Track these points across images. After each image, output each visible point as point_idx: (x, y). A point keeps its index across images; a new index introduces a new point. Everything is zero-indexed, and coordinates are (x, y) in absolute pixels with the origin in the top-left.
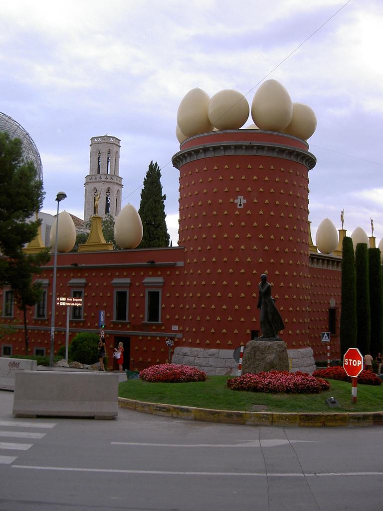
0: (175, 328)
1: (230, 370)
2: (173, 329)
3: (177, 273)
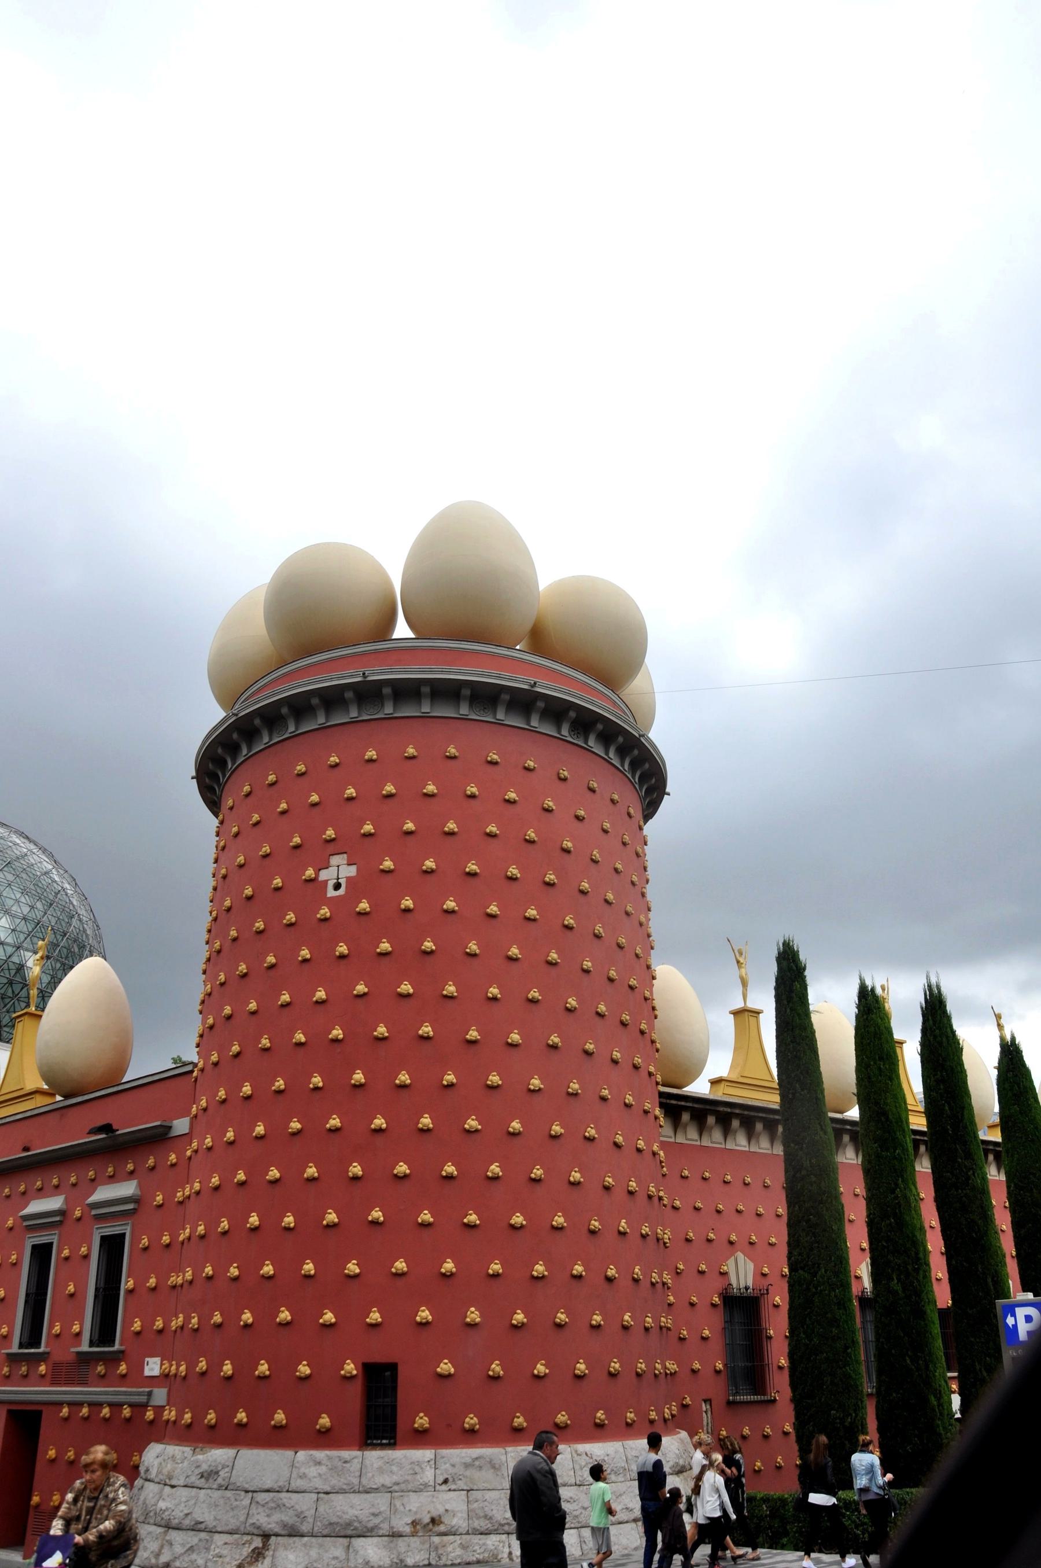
0: (153, 1367)
1: (258, 1542)
2: (147, 1372)
3: (173, 1158)
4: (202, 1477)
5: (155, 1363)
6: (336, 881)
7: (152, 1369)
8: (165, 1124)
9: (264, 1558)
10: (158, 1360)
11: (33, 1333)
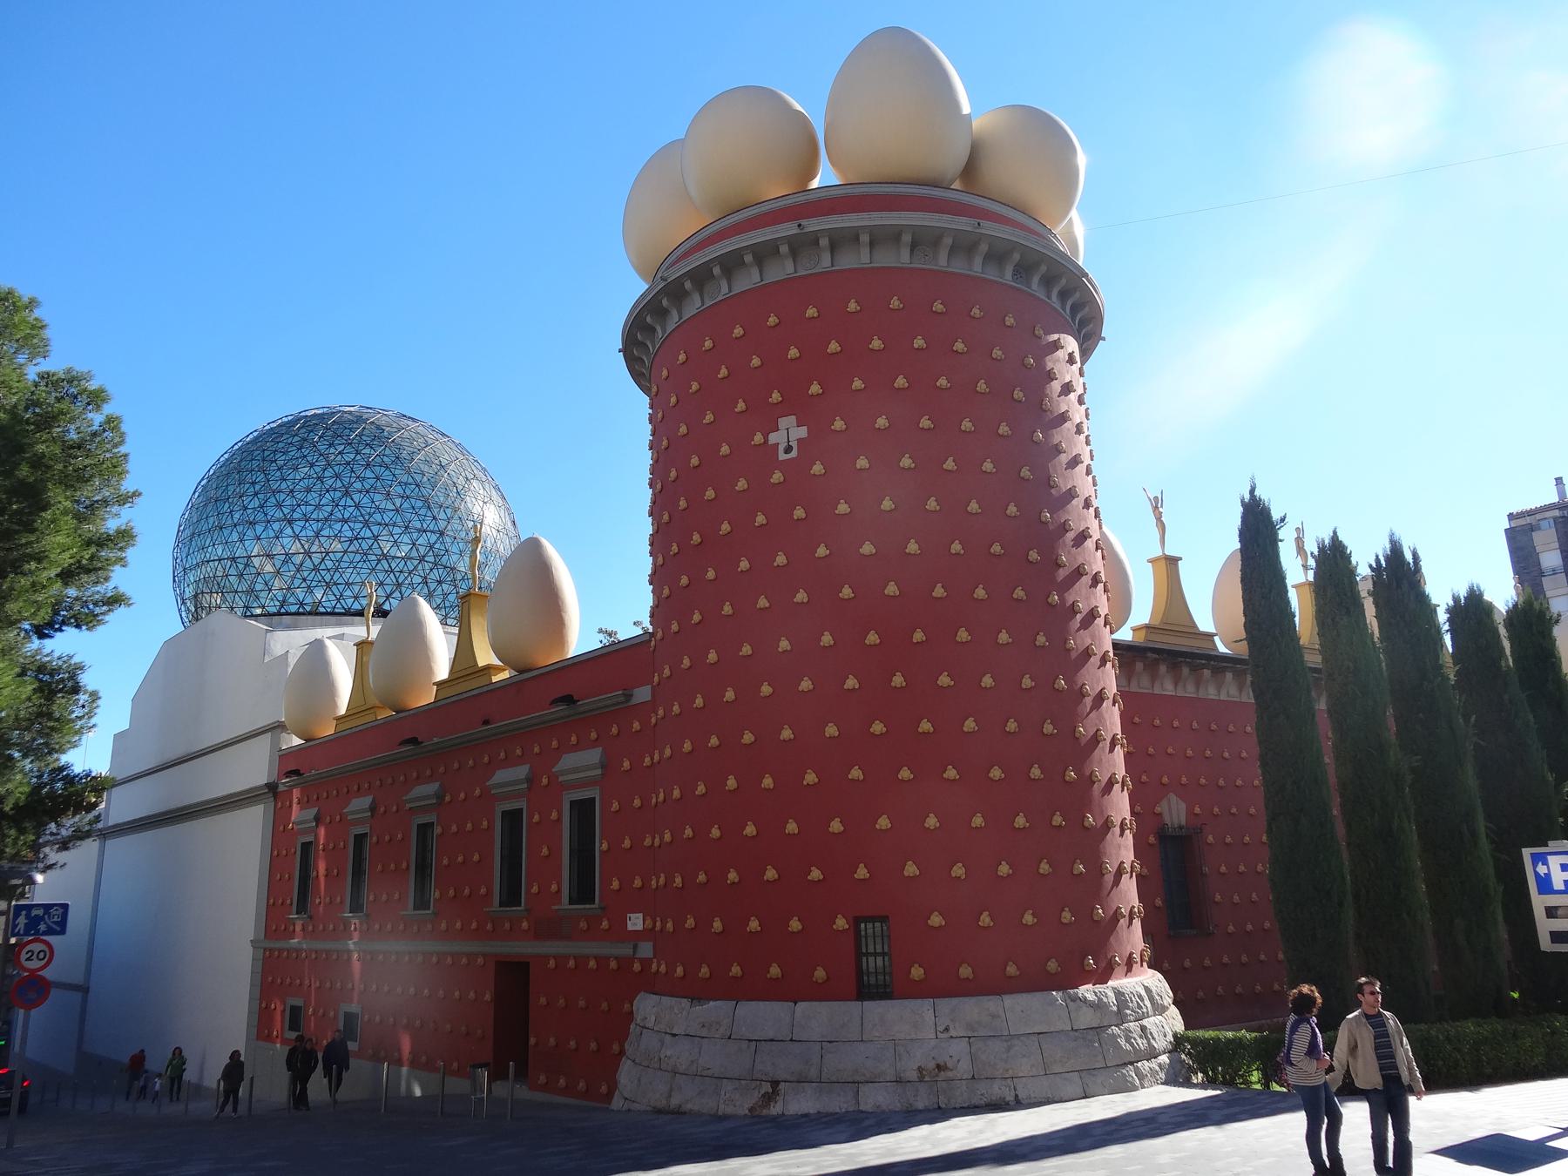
0: (636, 922)
1: (767, 1088)
2: (630, 927)
4: (703, 1026)
5: (638, 918)
6: (786, 444)
7: (635, 924)
8: (626, 692)
9: (776, 1102)
10: (640, 915)
11: (511, 895)
